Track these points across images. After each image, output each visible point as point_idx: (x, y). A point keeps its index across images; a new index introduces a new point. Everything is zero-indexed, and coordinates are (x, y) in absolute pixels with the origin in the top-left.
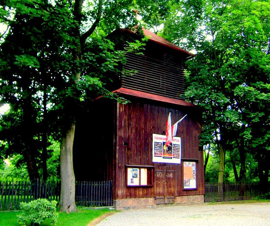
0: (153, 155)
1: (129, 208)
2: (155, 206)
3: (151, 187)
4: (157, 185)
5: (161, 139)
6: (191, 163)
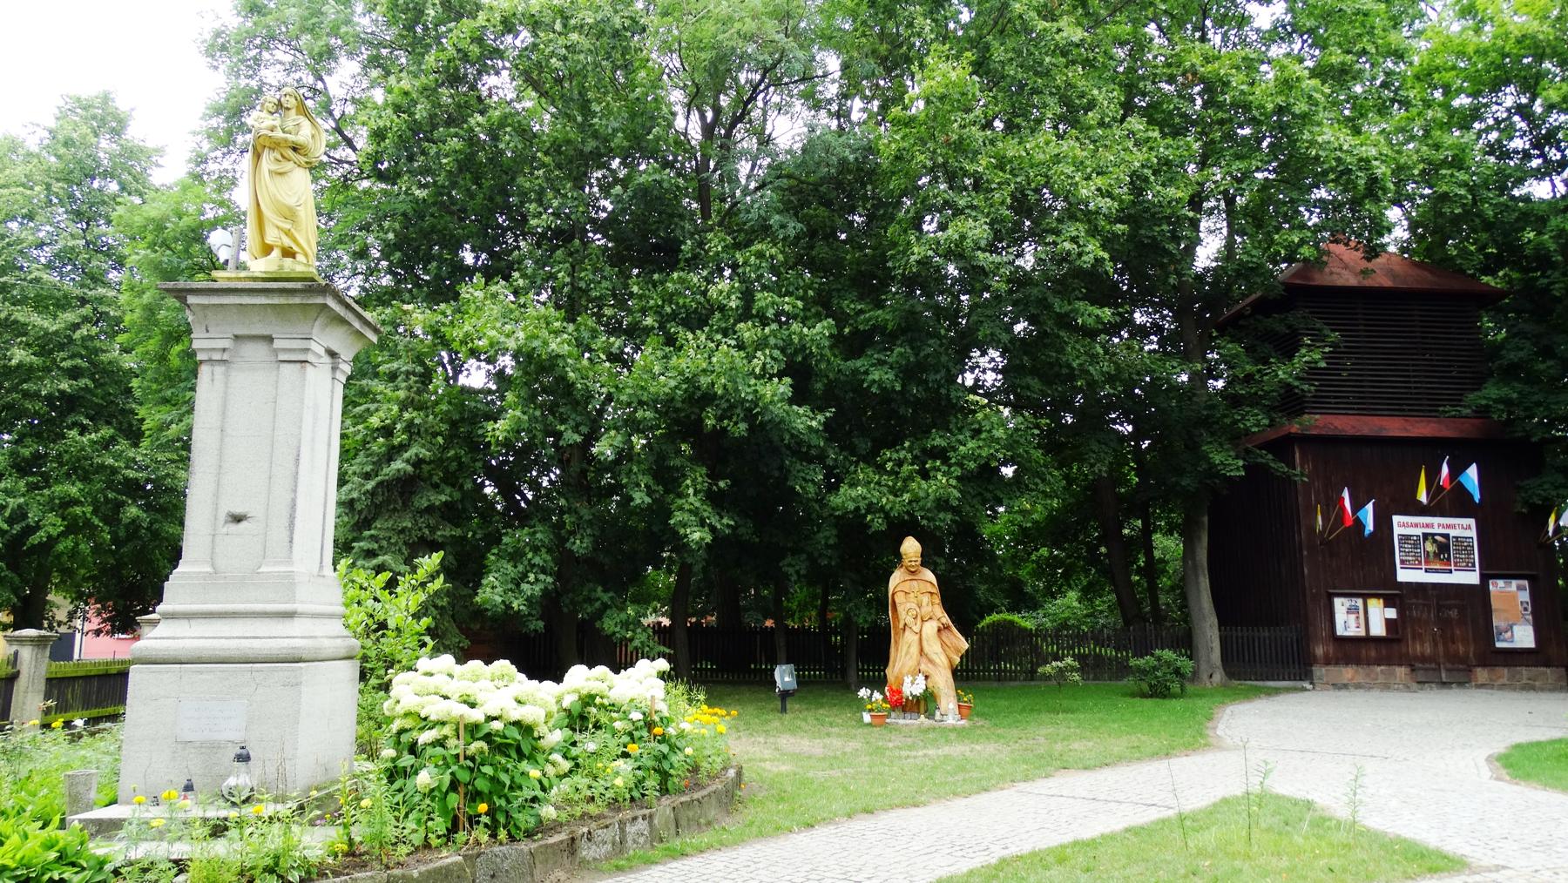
0: (1398, 565)
1: (1345, 686)
2: (1415, 685)
3: (1398, 641)
4: (1414, 638)
5: (1416, 525)
6: (1514, 583)
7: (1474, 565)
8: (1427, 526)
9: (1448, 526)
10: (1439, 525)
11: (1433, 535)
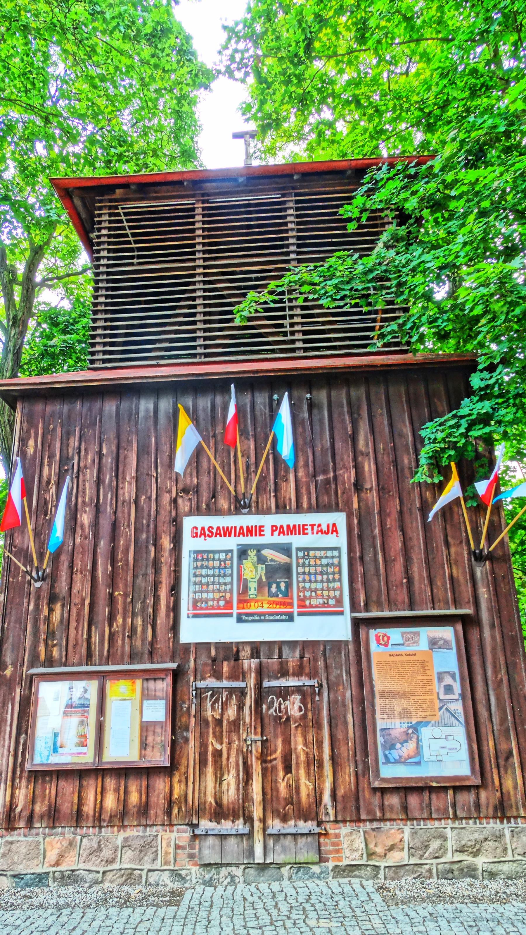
5: (227, 532)
7: (339, 601)
8: (250, 531)
9: (292, 530)
10: (274, 528)
11: (259, 548)
